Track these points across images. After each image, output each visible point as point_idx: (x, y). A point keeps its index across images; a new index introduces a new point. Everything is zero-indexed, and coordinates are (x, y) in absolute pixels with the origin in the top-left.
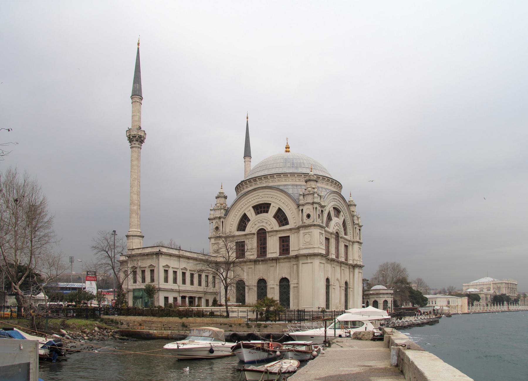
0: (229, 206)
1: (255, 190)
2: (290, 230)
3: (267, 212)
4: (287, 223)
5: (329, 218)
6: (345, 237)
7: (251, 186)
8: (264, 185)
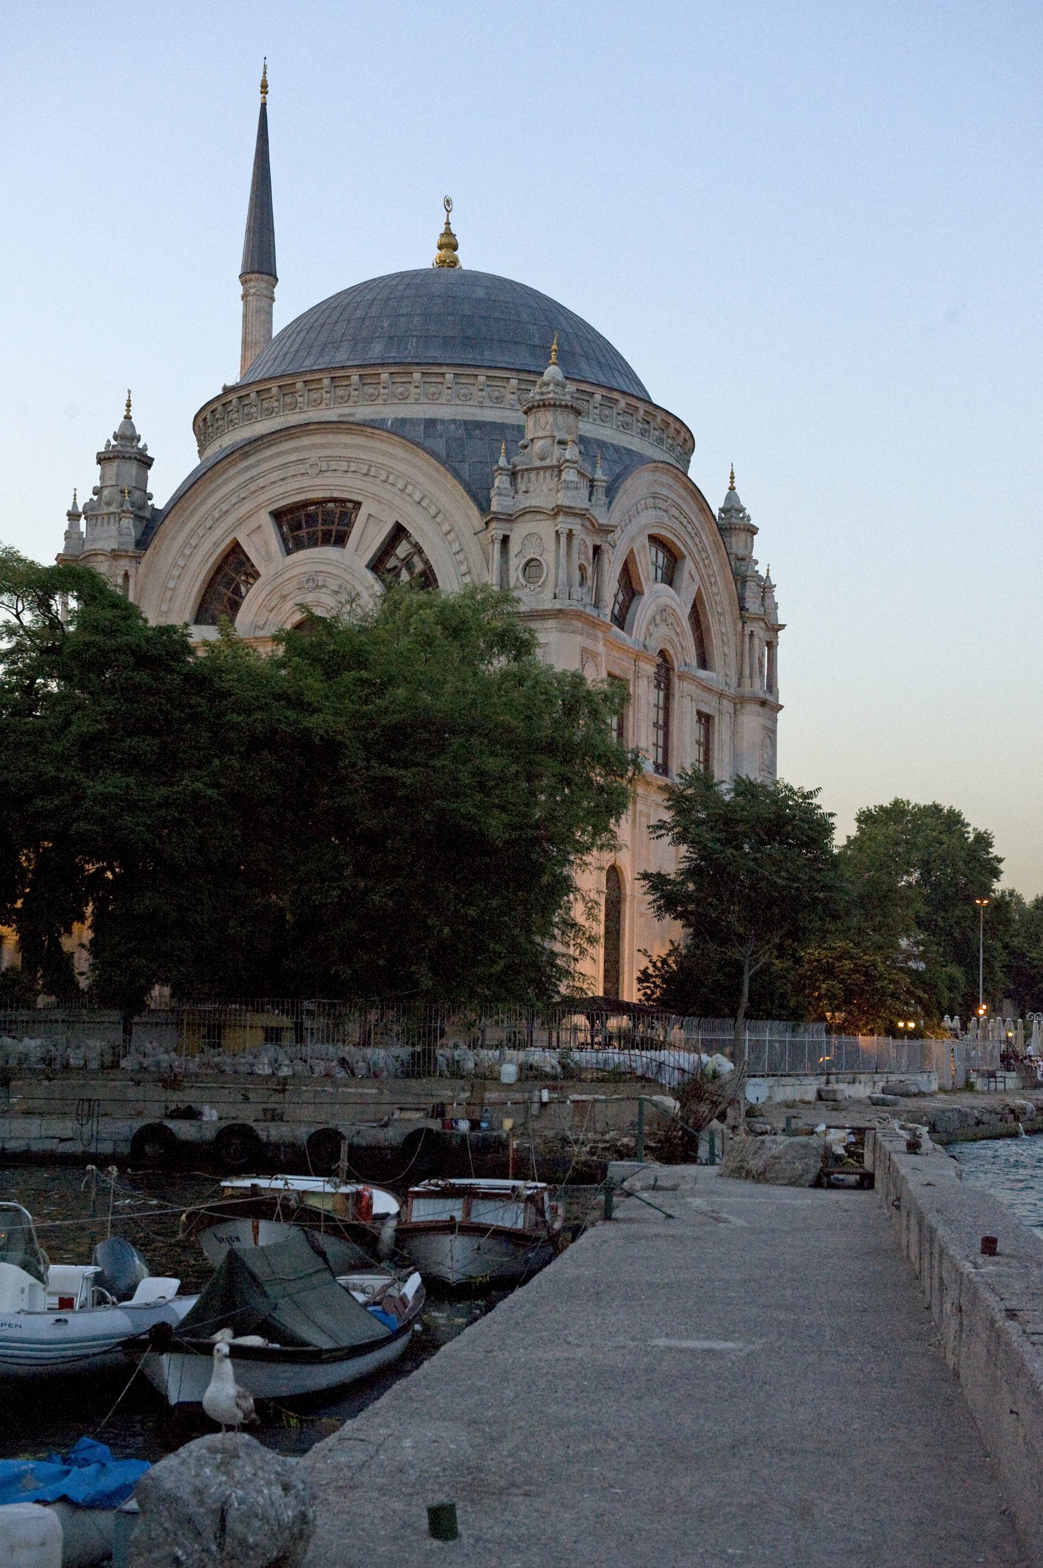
0: (160, 501)
3: (341, 540)
5: (630, 588)
6: (703, 674)
7: (270, 412)
8: (332, 415)
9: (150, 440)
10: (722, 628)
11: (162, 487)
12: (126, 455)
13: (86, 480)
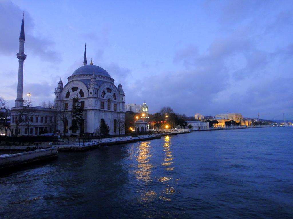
1: (72, 81)
2: (85, 98)
4: (84, 96)
8: (76, 79)
9: (63, 82)
10: (118, 96)
11: (64, 85)
12: (61, 83)
13: (57, 85)
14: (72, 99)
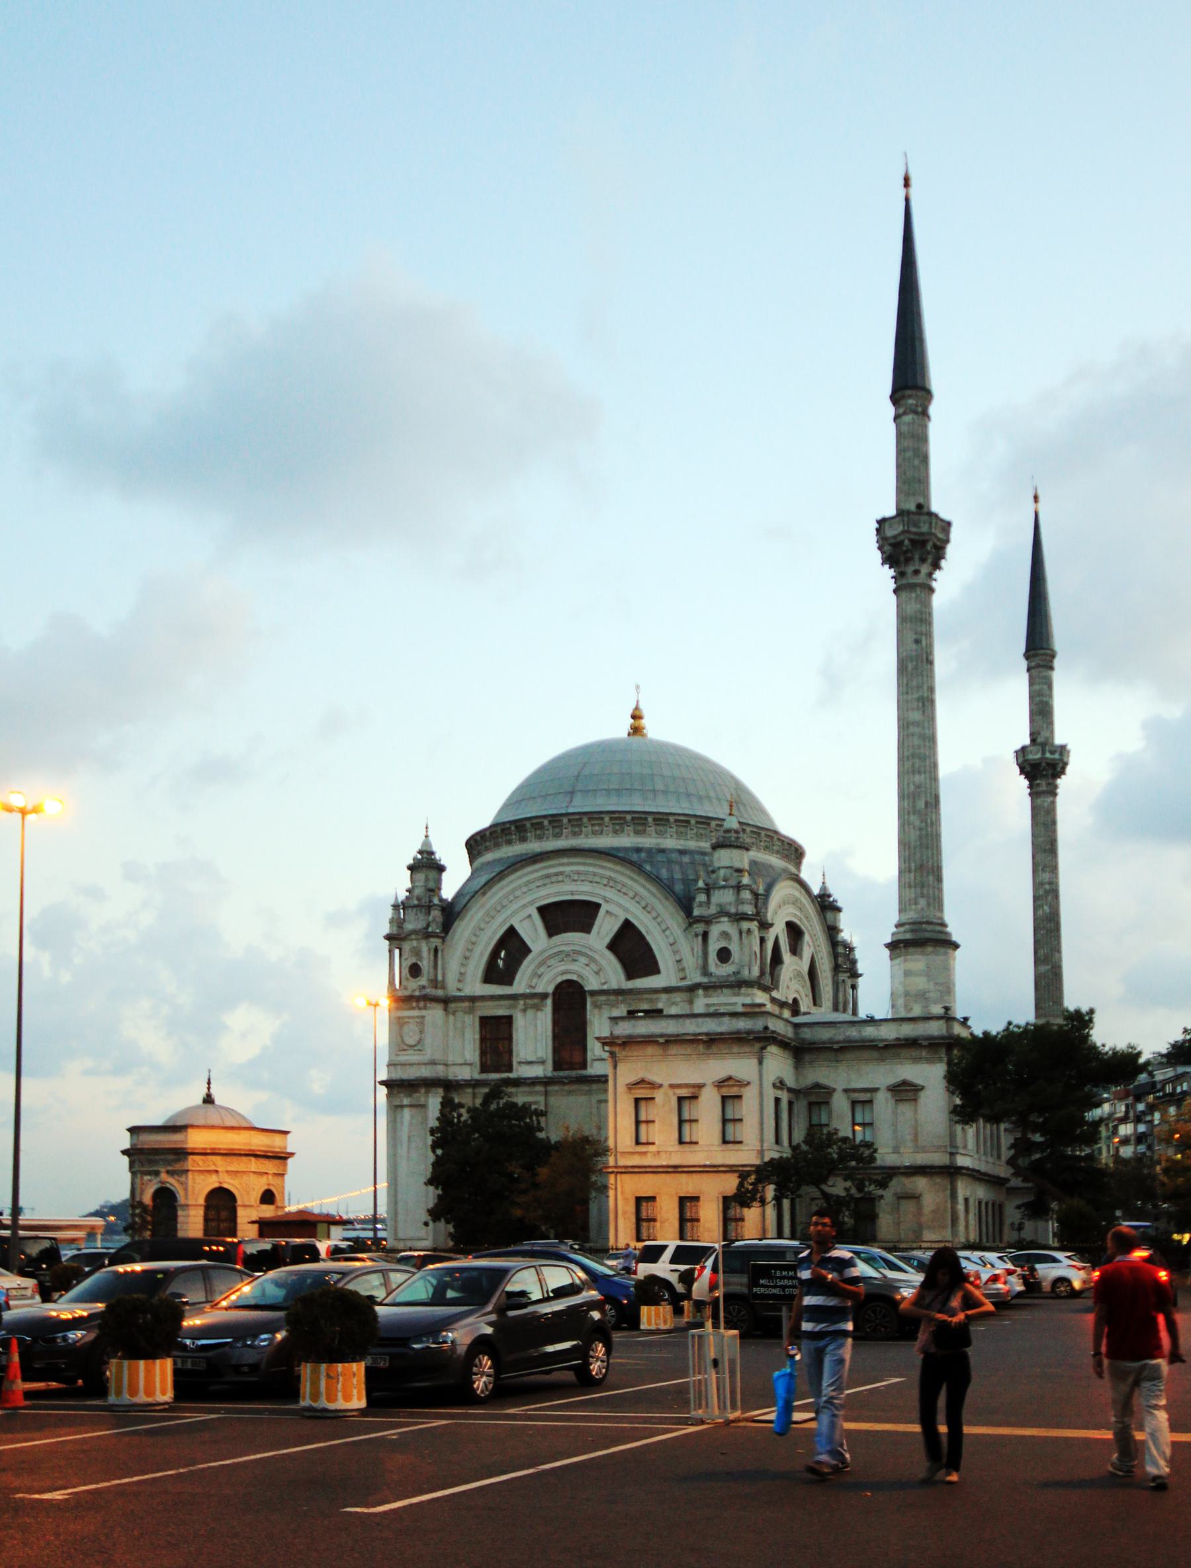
12: (426, 865)
13: (400, 884)
14: (547, 985)
